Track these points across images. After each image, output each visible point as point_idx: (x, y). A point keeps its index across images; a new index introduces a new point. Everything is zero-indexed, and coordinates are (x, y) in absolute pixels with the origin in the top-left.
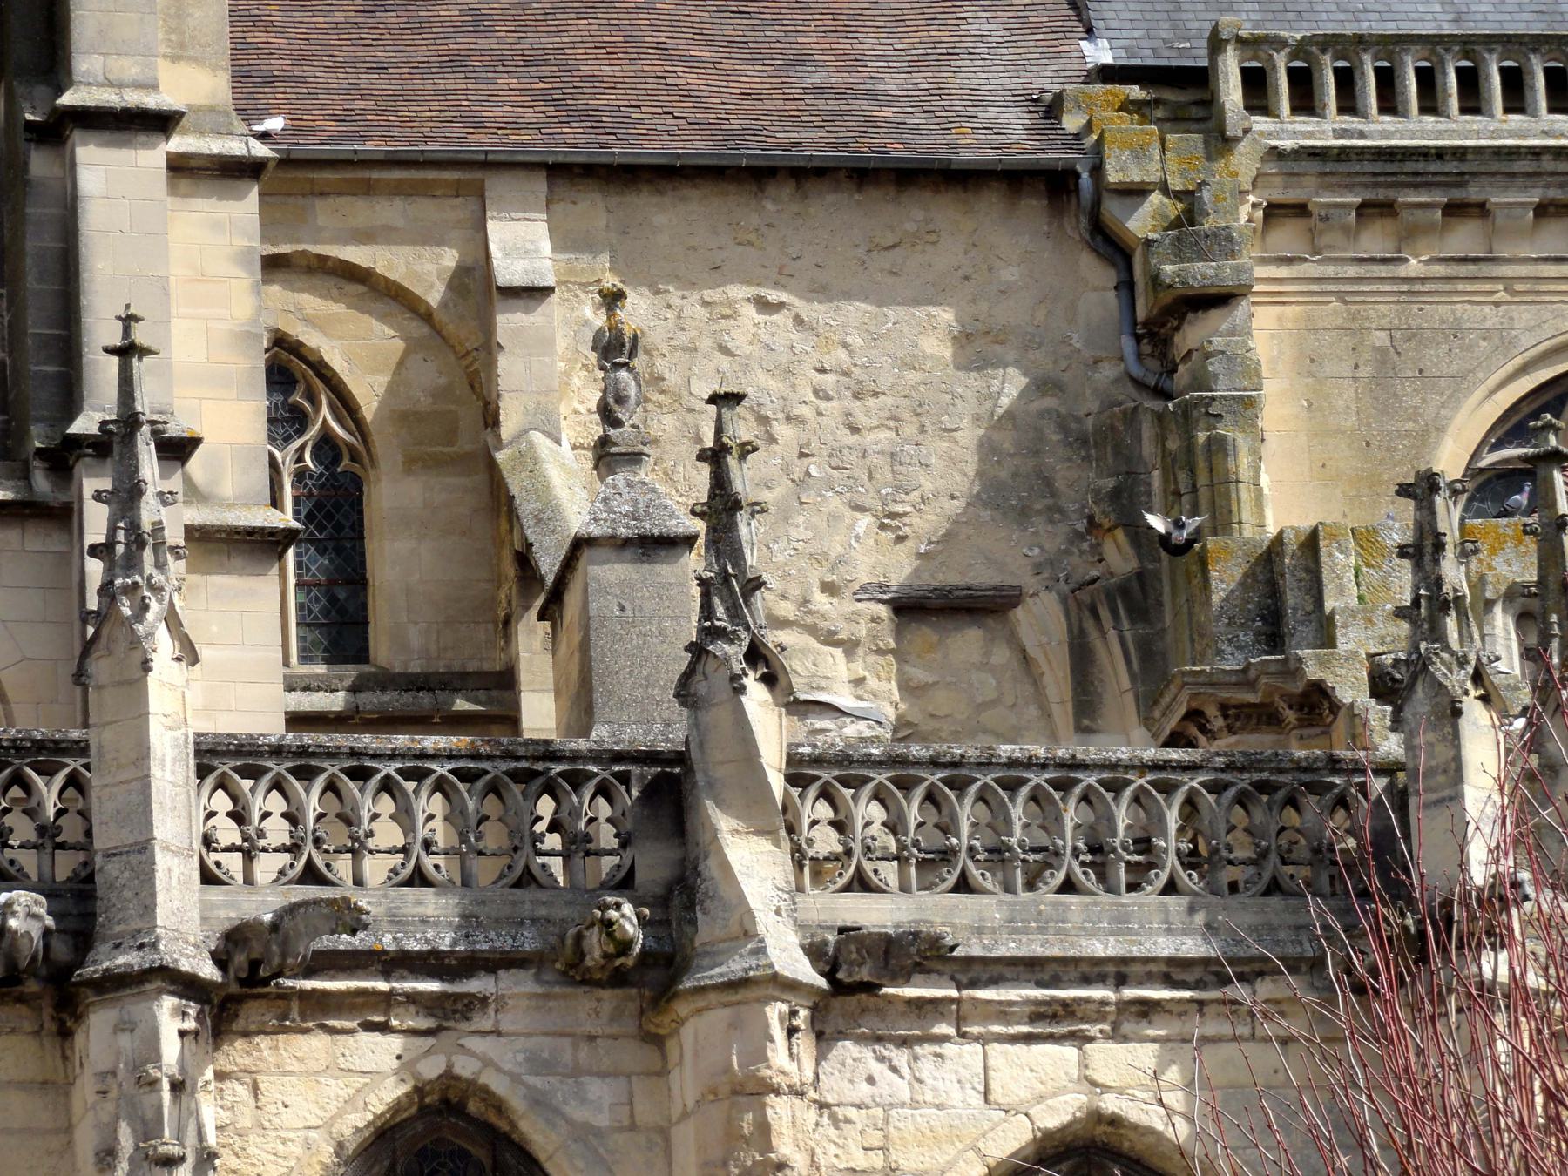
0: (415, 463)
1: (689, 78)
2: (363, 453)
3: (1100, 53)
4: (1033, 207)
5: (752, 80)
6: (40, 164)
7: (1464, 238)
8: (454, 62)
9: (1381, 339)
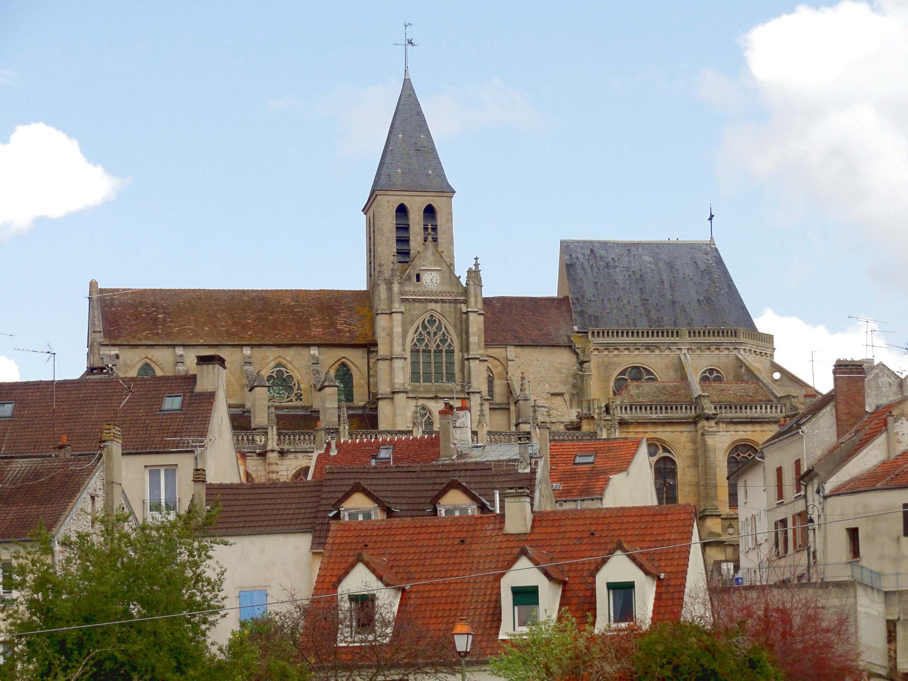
0: (499, 379)
1: (530, 332)
2: (493, 378)
3: (576, 328)
4: (568, 349)
5: (536, 332)
6: (466, 362)
7: (616, 352)
8: (503, 330)
9: (606, 364)
